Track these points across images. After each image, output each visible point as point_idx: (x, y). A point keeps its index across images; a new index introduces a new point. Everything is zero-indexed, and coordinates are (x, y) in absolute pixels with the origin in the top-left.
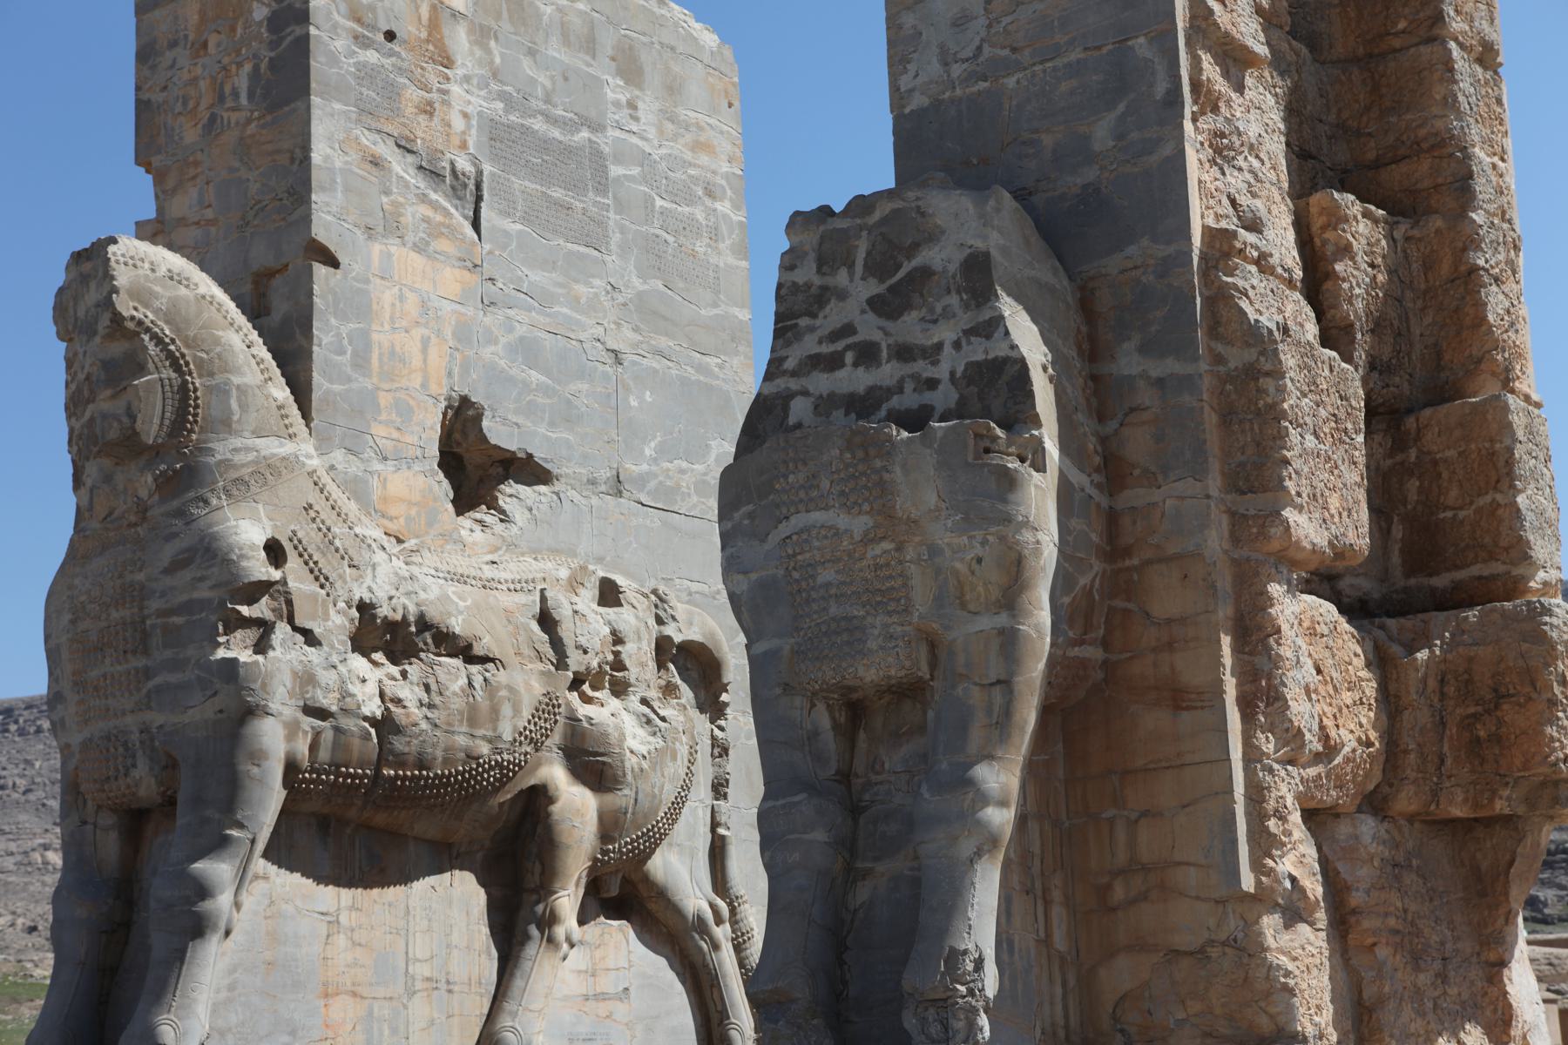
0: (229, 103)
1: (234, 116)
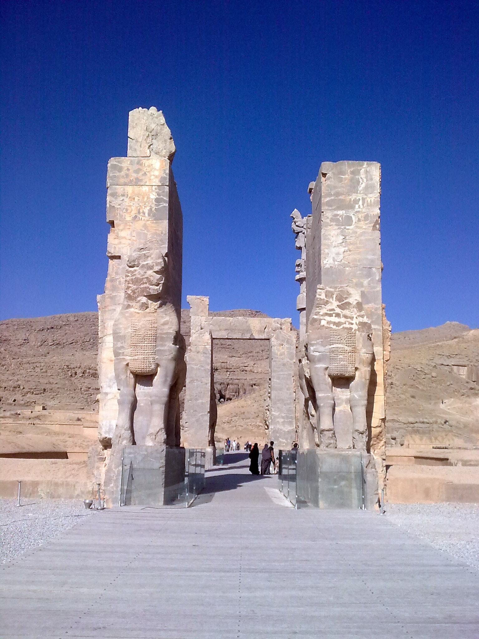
0: (141, 214)
1: (143, 218)
